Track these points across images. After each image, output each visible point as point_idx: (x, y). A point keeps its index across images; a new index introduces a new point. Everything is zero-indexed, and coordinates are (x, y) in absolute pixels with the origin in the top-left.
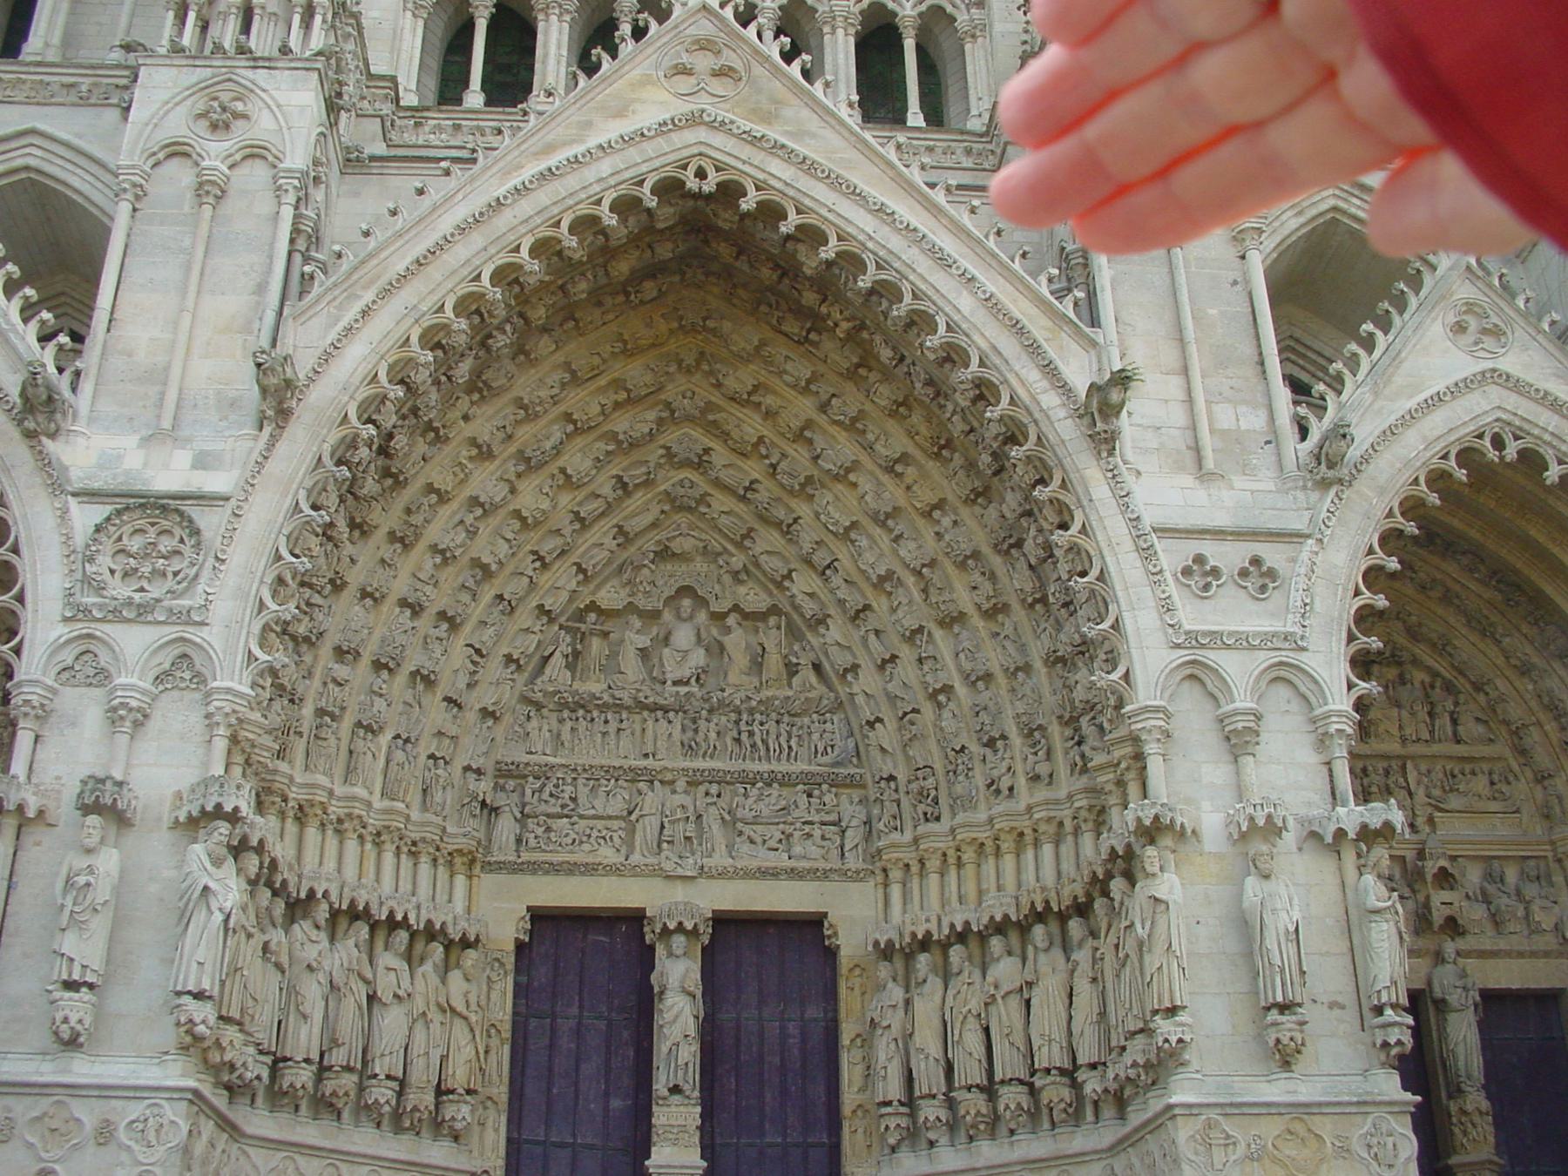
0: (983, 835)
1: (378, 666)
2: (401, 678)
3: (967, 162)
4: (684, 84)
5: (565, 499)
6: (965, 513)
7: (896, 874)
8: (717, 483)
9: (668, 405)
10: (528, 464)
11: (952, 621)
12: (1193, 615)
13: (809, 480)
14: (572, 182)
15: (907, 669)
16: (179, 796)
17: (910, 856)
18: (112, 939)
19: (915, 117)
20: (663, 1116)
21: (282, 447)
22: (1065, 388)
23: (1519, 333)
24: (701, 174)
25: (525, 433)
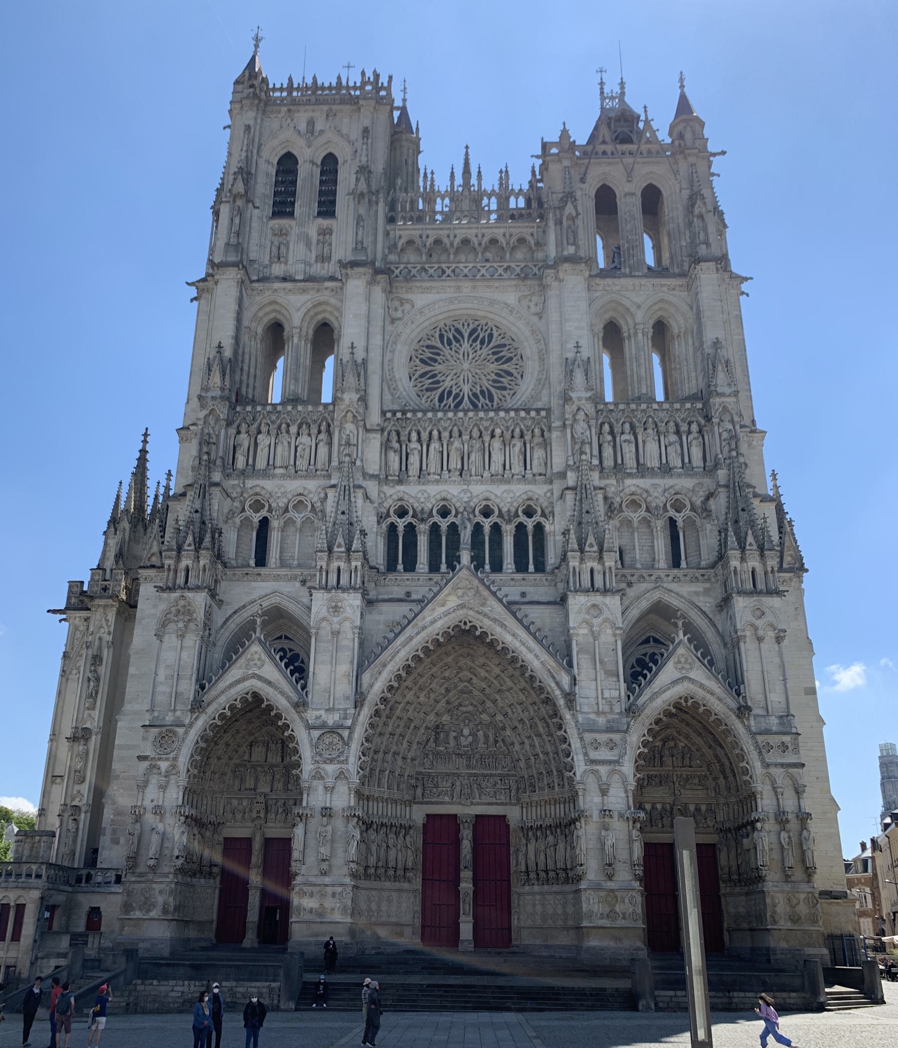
0: (546, 798)
1: (385, 753)
2: (390, 755)
3: (546, 583)
4: (460, 592)
5: (432, 696)
7: (525, 805)
9: (460, 668)
10: (421, 689)
11: (539, 735)
13: (499, 690)
14: (430, 629)
15: (527, 747)
16: (343, 809)
17: (528, 800)
18: (332, 847)
19: (531, 568)
21: (362, 713)
24: (465, 623)
25: (421, 681)
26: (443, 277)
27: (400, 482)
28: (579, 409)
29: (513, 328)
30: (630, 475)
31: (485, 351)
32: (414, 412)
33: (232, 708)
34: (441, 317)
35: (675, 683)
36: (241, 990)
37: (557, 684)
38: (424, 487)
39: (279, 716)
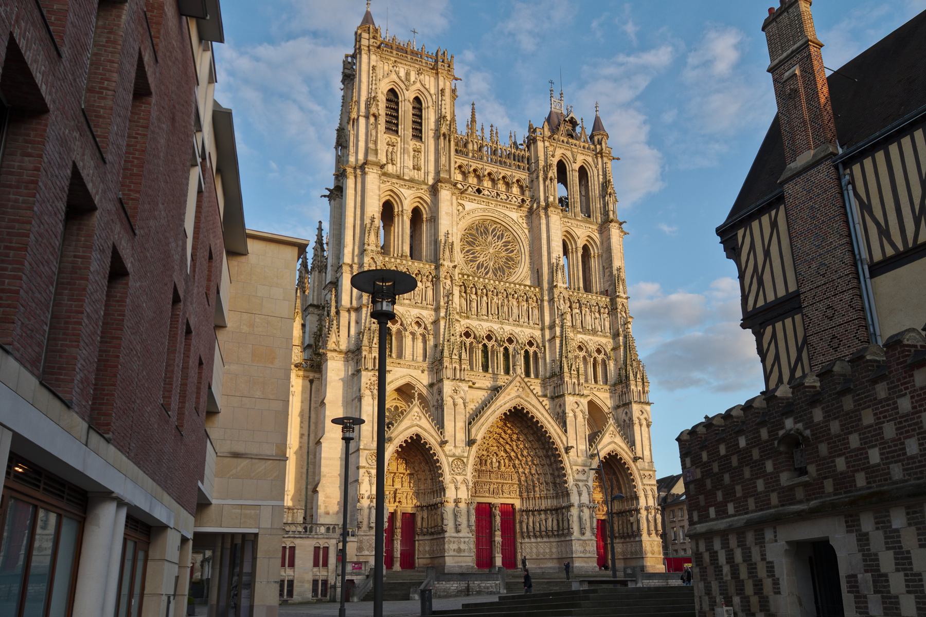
6: (540, 450)
8: (503, 438)
12: (576, 477)
14: (503, 407)
19: (532, 376)
20: (496, 533)
22: (563, 443)
23: (618, 435)
26: (481, 195)
27: (468, 318)
28: (561, 293)
29: (515, 234)
30: (580, 332)
31: (500, 243)
32: (473, 277)
33: (406, 441)
34: (478, 218)
35: (609, 444)
36: (483, 585)
37: (562, 441)
38: (480, 323)
39: (430, 448)
